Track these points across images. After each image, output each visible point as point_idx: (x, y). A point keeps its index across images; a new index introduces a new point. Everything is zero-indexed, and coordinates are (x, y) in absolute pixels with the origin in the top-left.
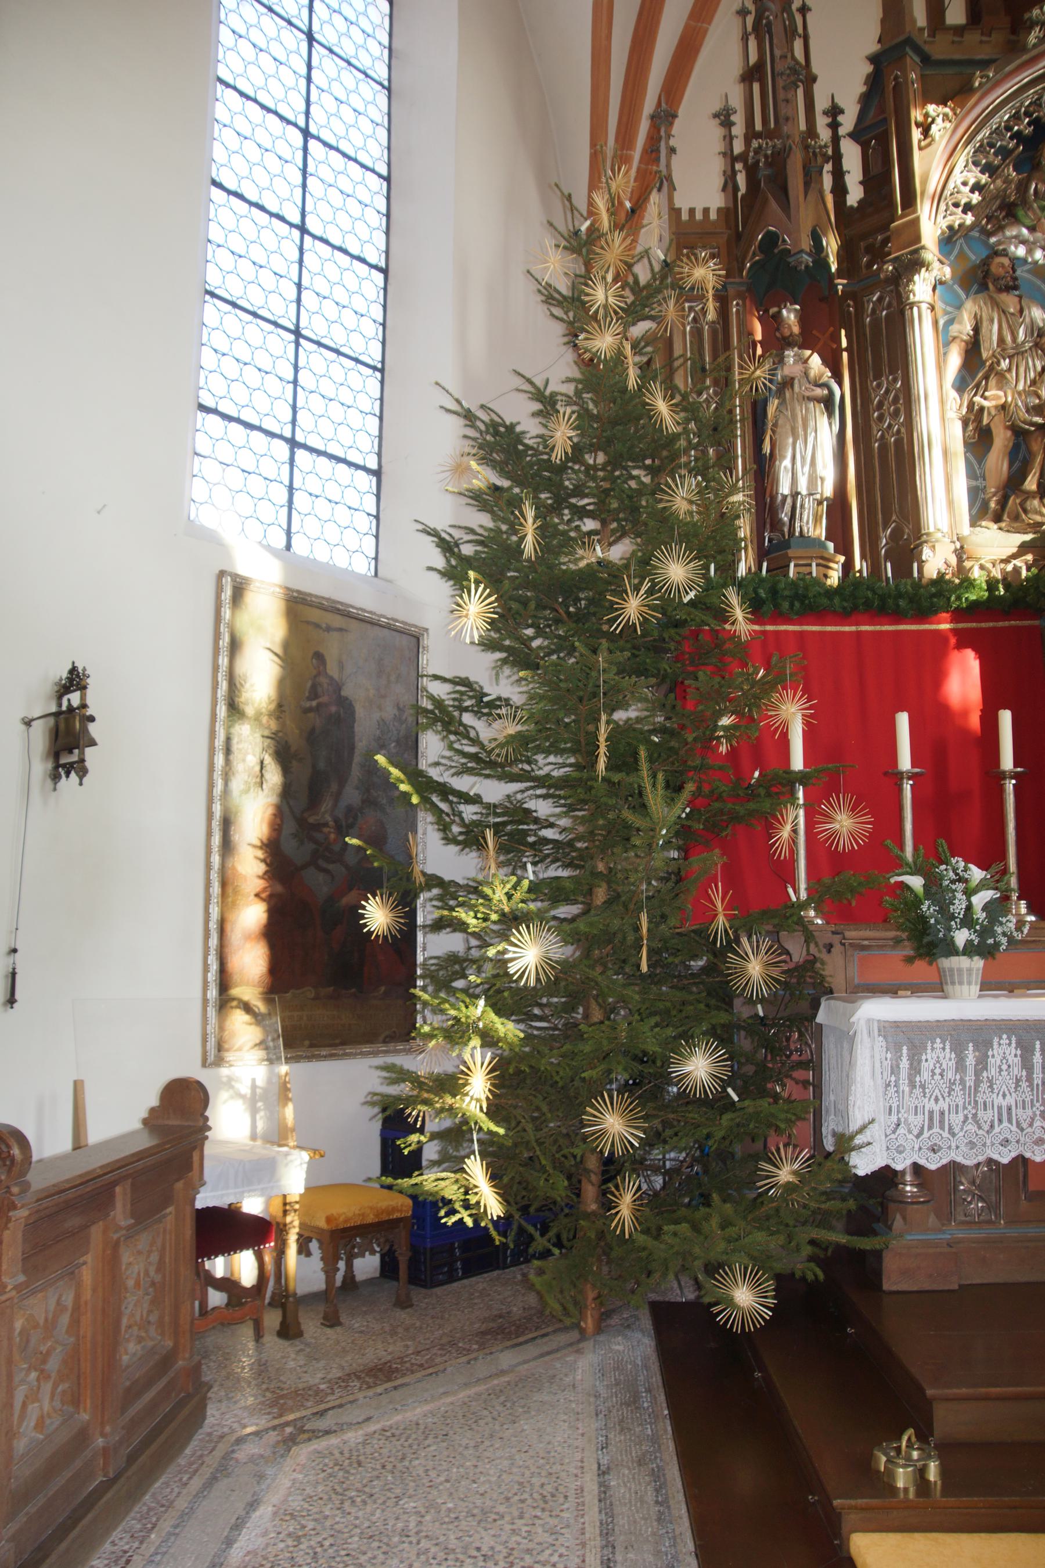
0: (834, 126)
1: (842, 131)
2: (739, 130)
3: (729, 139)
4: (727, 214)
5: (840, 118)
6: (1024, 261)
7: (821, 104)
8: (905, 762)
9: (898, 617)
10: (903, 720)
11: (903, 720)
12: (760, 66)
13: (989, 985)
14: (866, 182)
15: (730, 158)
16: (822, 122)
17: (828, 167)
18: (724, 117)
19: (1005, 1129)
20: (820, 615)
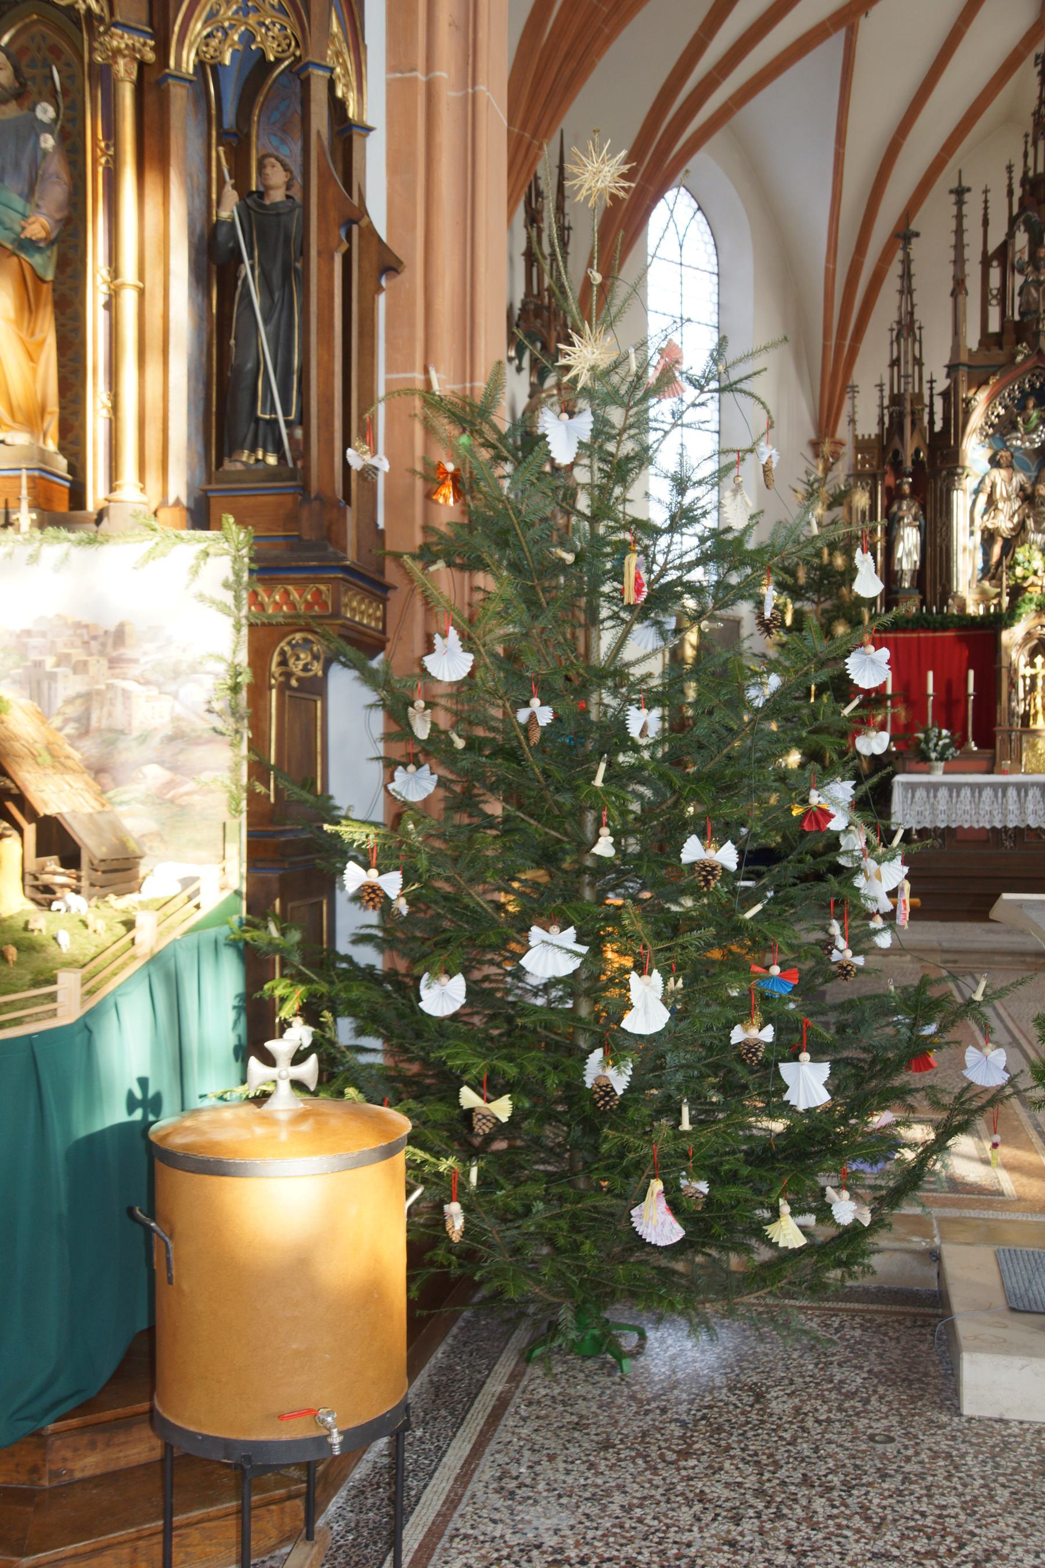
0: (931, 389)
1: (935, 392)
2: (887, 393)
3: (882, 397)
4: (879, 437)
6: (1020, 448)
7: (926, 377)
8: (930, 690)
9: (935, 630)
10: (930, 675)
11: (930, 675)
12: (898, 359)
13: (945, 773)
14: (946, 419)
15: (881, 407)
16: (926, 386)
17: (927, 410)
18: (881, 386)
19: (943, 817)
20: (904, 631)
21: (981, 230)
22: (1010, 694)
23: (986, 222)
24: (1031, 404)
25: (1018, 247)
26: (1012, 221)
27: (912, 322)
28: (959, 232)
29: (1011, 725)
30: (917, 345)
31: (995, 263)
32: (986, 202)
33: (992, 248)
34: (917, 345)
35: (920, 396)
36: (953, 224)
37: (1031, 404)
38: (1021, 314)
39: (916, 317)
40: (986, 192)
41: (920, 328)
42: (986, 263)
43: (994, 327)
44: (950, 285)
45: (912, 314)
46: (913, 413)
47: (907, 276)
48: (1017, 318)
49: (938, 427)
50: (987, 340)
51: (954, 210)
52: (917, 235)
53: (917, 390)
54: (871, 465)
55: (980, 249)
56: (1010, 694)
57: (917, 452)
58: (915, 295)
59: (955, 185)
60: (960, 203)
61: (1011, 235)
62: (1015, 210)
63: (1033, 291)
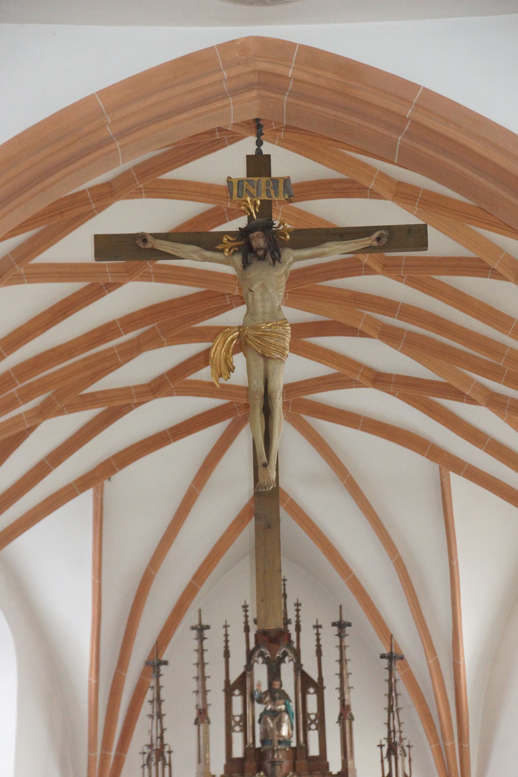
21: (223, 660)
23: (227, 654)
25: (256, 678)
26: (250, 655)
27: (163, 745)
28: (201, 664)
30: (167, 768)
31: (237, 692)
32: (226, 635)
33: (233, 678)
34: (167, 768)
36: (195, 658)
38: (263, 742)
39: (165, 741)
40: (226, 626)
41: (170, 752)
43: (238, 752)
44: (194, 714)
45: (161, 738)
47: (158, 701)
48: (258, 745)
51: (195, 644)
52: (166, 663)
55: (223, 677)
58: (165, 719)
59: (196, 623)
60: (201, 638)
61: (249, 667)
62: (252, 645)
63: (269, 720)
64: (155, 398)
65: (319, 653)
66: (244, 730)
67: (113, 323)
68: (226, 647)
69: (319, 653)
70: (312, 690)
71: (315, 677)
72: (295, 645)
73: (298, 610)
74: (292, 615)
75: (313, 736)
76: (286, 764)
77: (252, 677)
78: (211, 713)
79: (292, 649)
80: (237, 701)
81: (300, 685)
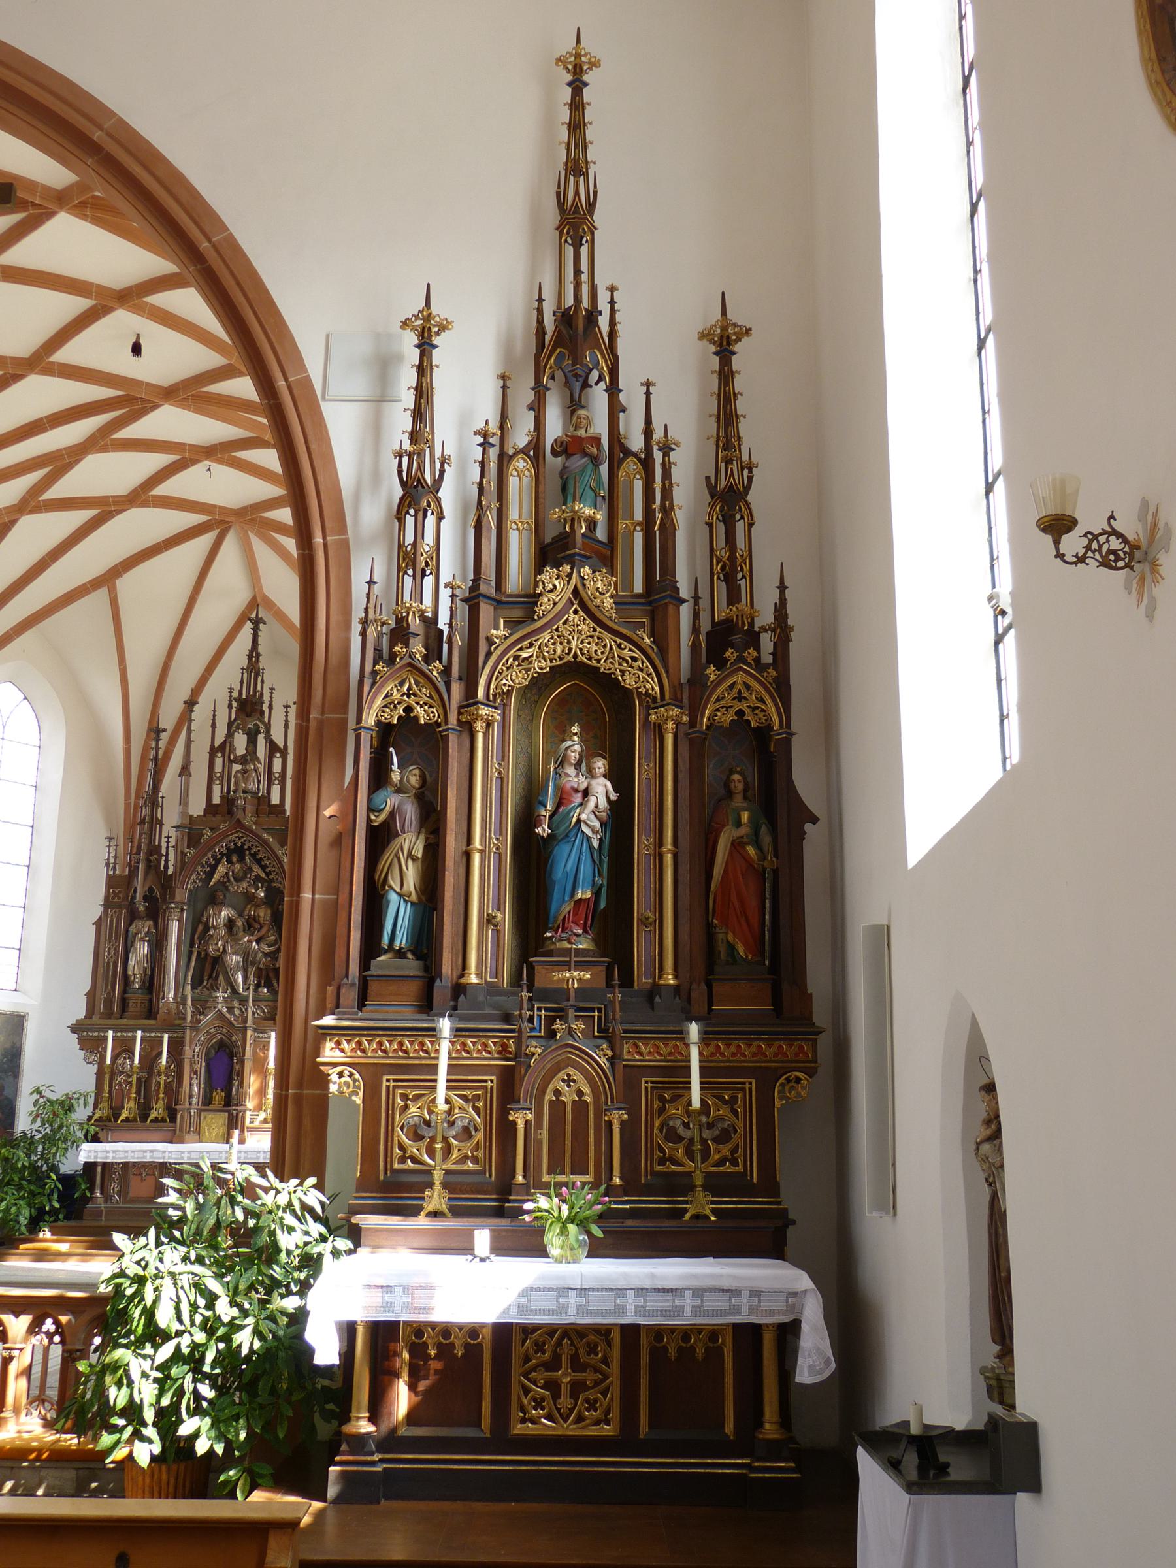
0: (168, 842)
1: (170, 845)
5: (170, 839)
7: (164, 834)
17: (164, 858)
22: (191, 1079)
23: (214, 726)
24: (234, 859)
26: (230, 724)
29: (190, 1104)
30: (160, 809)
31: (219, 755)
33: (216, 745)
35: (160, 846)
37: (234, 859)
41: (162, 797)
42: (213, 752)
43: (216, 800)
46: (148, 861)
49: (170, 872)
50: (210, 808)
53: (157, 844)
54: (119, 898)
56: (191, 1079)
57: (151, 890)
61: (230, 735)
64: (132, 507)
65: (286, 726)
66: (222, 784)
67: (41, 419)
68: (214, 720)
69: (286, 726)
70: (278, 755)
71: (281, 746)
72: (266, 720)
73: (272, 693)
74: (266, 699)
75: (276, 790)
76: (249, 808)
77: (231, 743)
78: (192, 768)
79: (263, 723)
80: (219, 761)
81: (268, 750)
